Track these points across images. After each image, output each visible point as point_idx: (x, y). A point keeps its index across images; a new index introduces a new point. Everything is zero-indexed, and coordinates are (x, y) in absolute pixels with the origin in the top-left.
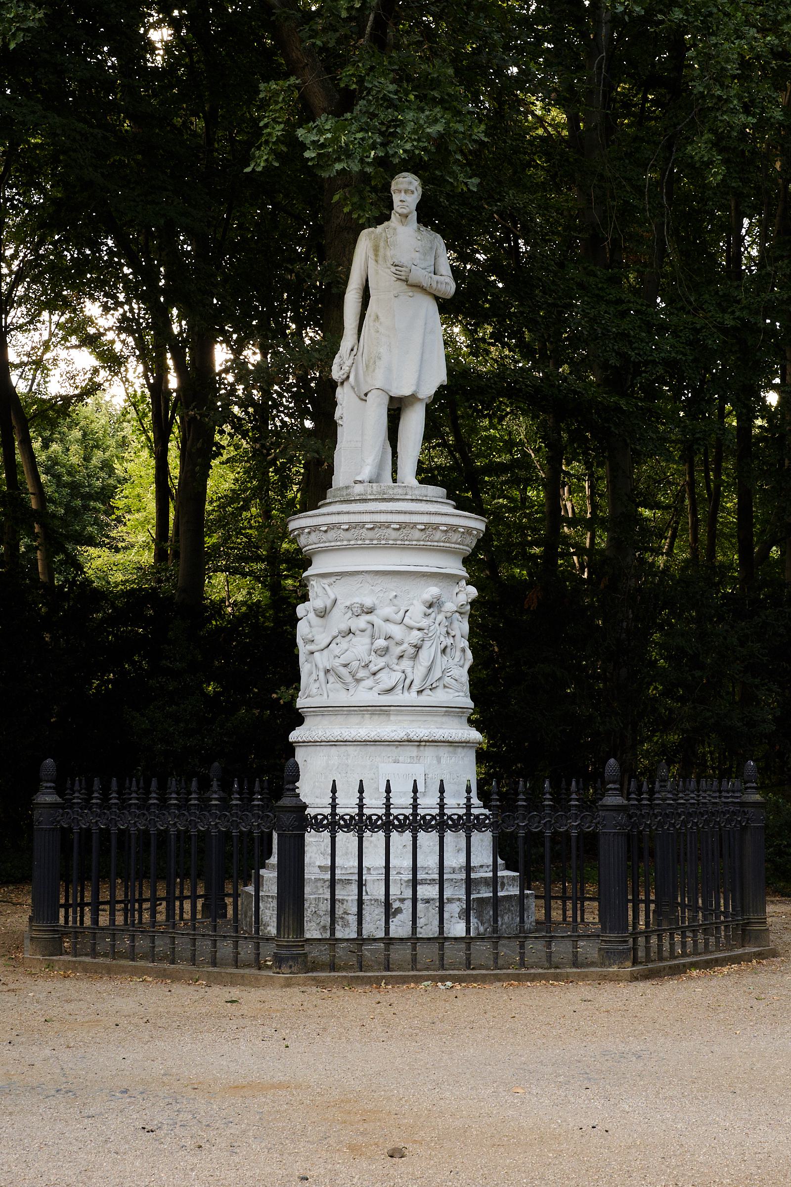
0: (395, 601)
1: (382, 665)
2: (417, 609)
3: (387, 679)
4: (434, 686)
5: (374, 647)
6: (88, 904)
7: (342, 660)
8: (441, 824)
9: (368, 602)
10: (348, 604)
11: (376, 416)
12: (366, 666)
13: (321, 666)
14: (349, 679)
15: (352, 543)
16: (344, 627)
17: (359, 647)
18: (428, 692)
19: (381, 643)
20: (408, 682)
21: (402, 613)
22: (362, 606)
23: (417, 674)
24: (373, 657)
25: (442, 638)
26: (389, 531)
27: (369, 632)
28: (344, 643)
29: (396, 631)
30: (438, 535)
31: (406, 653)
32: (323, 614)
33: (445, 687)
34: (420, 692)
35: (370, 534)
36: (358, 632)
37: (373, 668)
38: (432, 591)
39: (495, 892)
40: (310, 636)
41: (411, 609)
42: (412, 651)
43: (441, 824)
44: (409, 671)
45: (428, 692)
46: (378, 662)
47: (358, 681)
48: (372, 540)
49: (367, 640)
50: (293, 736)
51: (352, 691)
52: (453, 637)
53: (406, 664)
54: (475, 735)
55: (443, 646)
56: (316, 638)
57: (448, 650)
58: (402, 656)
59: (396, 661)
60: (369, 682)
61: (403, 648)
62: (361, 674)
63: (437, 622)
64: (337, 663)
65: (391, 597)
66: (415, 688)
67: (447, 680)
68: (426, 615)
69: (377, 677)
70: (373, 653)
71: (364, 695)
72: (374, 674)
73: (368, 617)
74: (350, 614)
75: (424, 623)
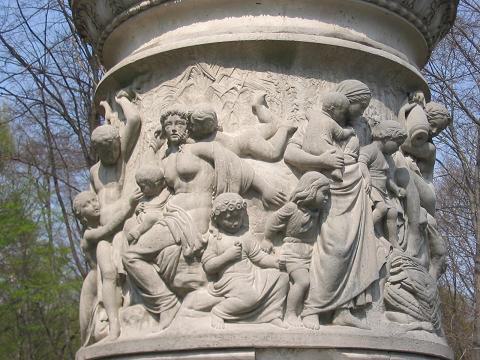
3: (247, 283)
4: (360, 302)
7: (144, 245)
14: (160, 289)
17: (184, 215)
18: (347, 316)
20: (296, 289)
21: (280, 136)
25: (376, 195)
28: (150, 209)
31: (293, 223)
34: (326, 318)
37: (211, 259)
40: (89, 208)
47: (181, 293)
51: (165, 317)
59: (268, 244)
61: (281, 212)
62: (182, 276)
65: (255, 102)
67: (388, 290)
68: (340, 140)
72: (215, 274)
73: (203, 146)
75: (330, 154)
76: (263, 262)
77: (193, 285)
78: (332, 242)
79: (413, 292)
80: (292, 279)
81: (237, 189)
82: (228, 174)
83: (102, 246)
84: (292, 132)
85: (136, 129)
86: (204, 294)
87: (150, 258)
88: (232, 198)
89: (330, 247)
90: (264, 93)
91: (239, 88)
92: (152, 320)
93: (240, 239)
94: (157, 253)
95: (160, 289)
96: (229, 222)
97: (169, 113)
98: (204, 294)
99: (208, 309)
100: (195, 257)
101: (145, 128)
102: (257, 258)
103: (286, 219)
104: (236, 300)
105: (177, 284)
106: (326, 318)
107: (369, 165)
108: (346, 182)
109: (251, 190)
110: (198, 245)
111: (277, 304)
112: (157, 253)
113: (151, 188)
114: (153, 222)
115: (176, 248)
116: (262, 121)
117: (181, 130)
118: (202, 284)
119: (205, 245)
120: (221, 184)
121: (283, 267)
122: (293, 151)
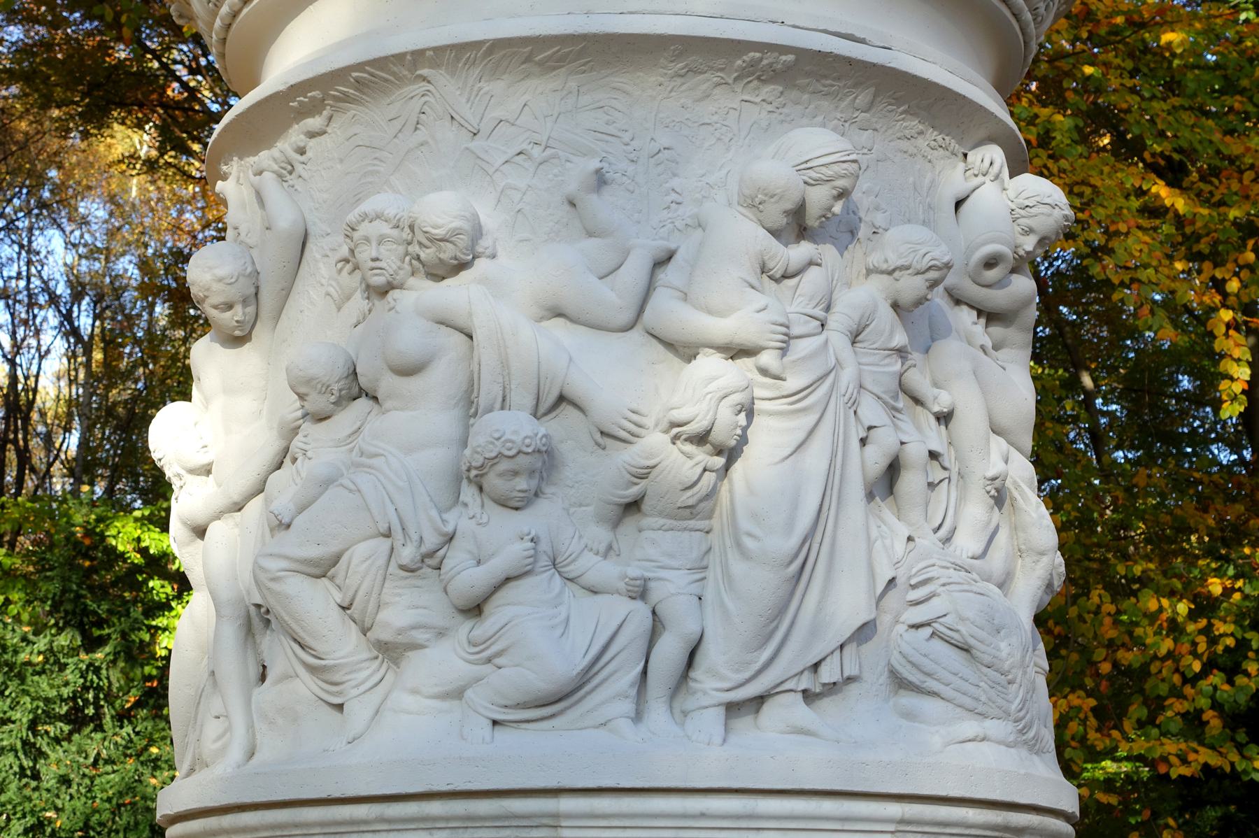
0: (602, 207)
1: (511, 553)
3: (546, 633)
4: (829, 674)
12: (431, 561)
14: (342, 644)
20: (669, 650)
21: (634, 272)
25: (871, 411)
33: (900, 683)
36: (388, 383)
37: (467, 576)
38: (807, 147)
44: (673, 589)
45: (786, 711)
46: (494, 538)
47: (391, 652)
52: (945, 418)
55: (876, 458)
57: (911, 482)
58: (633, 506)
59: (600, 534)
62: (401, 610)
63: (839, 321)
65: (572, 187)
67: (899, 639)
72: (475, 610)
76: (591, 578)
77: (420, 636)
78: (757, 532)
80: (657, 626)
81: (529, 402)
82: (505, 364)
84: (663, 261)
86: (444, 660)
87: (323, 569)
88: (515, 426)
89: (749, 543)
90: (594, 164)
91: (536, 152)
93: (527, 521)
95: (342, 644)
97: (364, 217)
98: (444, 660)
102: (572, 570)
105: (386, 636)
107: (855, 337)
116: (590, 234)
117: (391, 259)
118: (441, 633)
120: (488, 391)
121: (640, 592)
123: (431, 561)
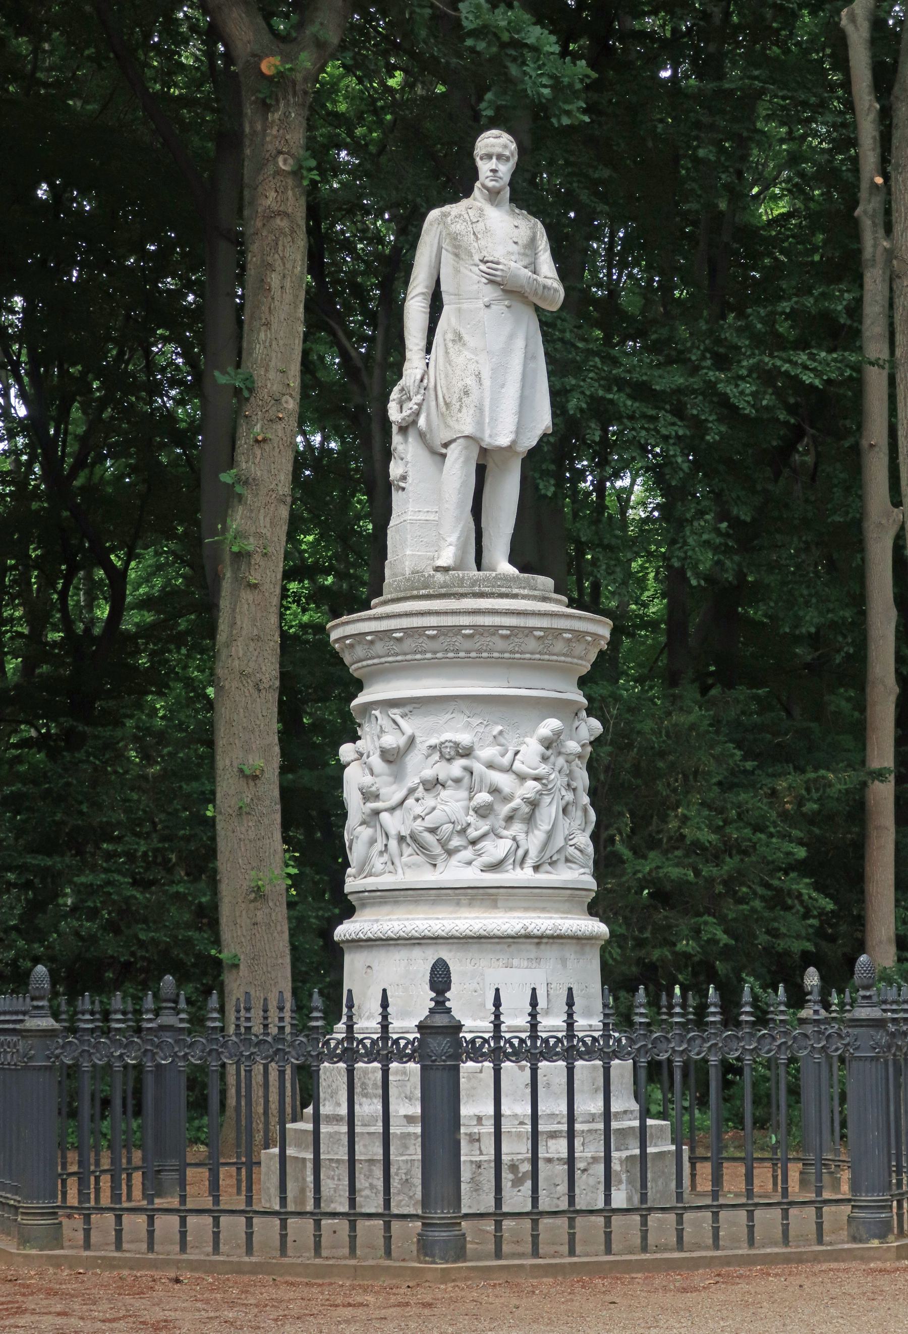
0: (501, 740)
1: (485, 828)
2: (531, 748)
3: (496, 849)
4: (554, 858)
5: (474, 803)
6: (137, 1168)
7: (429, 822)
8: (570, 1049)
9: (464, 738)
10: (434, 741)
11: (457, 472)
13: (393, 832)
14: (438, 850)
15: (439, 655)
16: (428, 773)
17: (451, 805)
19: (483, 797)
20: (520, 852)
21: (510, 755)
22: (457, 745)
23: (533, 842)
24: (472, 818)
26: (496, 639)
27: (466, 780)
29: (504, 781)
30: (559, 646)
31: (520, 812)
32: (393, 758)
33: (567, 860)
35: (468, 644)
37: (473, 833)
39: (643, 1146)
40: (374, 789)
41: (523, 749)
42: (526, 809)
43: (570, 1049)
44: (521, 837)
47: (450, 853)
48: (468, 652)
49: (464, 794)
50: (344, 931)
51: (440, 867)
53: (517, 828)
54: (599, 928)
56: (383, 791)
57: (570, 807)
59: (503, 824)
60: (468, 854)
62: (456, 842)
63: (557, 768)
64: (418, 825)
65: (495, 732)
66: (530, 862)
68: (545, 759)
69: (478, 847)
70: (471, 813)
71: (457, 872)
72: (474, 843)
74: (436, 756)
75: (543, 769)
79: (581, 851)
83: (384, 816)
84: (517, 753)
85: (412, 741)
92: (431, 868)
94: (437, 828)
96: (483, 812)
99: (469, 863)
100: (463, 831)
101: (418, 740)
103: (515, 810)
104: (486, 859)
106: (536, 868)
108: (550, 787)
109: (495, 790)
110: (465, 825)
111: (511, 861)
112: (437, 828)
113: (433, 785)
114: (434, 809)
115: (451, 826)
119: (469, 825)
121: (514, 839)
122: (517, 766)
123: (463, 831)
